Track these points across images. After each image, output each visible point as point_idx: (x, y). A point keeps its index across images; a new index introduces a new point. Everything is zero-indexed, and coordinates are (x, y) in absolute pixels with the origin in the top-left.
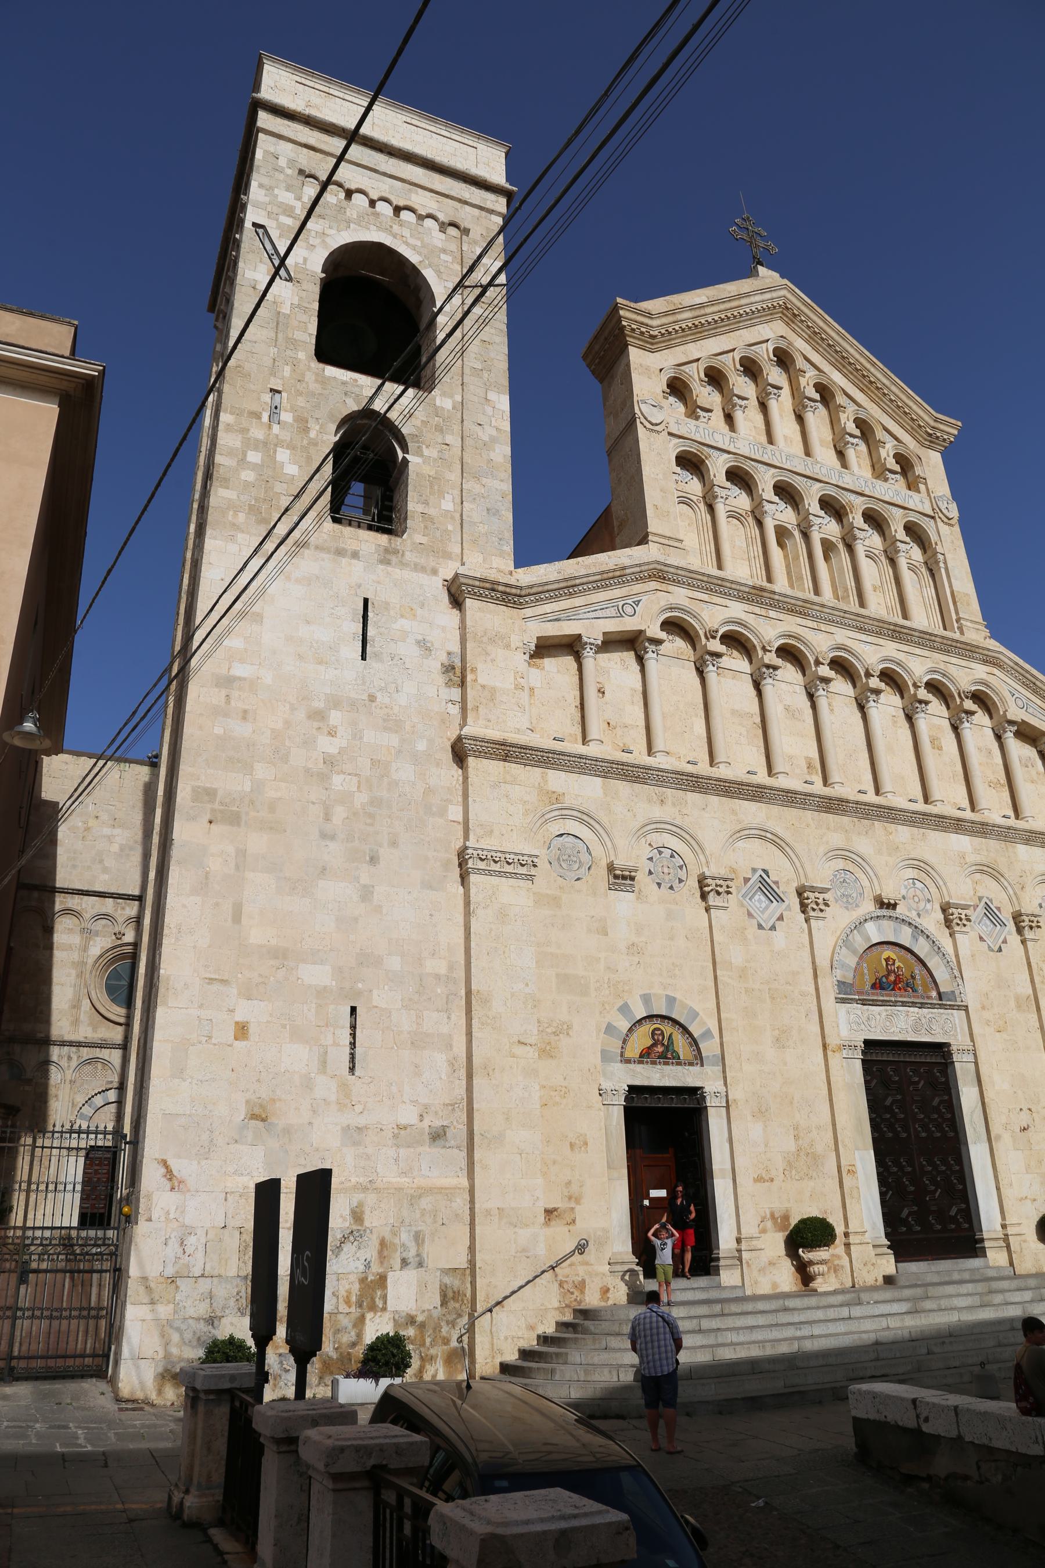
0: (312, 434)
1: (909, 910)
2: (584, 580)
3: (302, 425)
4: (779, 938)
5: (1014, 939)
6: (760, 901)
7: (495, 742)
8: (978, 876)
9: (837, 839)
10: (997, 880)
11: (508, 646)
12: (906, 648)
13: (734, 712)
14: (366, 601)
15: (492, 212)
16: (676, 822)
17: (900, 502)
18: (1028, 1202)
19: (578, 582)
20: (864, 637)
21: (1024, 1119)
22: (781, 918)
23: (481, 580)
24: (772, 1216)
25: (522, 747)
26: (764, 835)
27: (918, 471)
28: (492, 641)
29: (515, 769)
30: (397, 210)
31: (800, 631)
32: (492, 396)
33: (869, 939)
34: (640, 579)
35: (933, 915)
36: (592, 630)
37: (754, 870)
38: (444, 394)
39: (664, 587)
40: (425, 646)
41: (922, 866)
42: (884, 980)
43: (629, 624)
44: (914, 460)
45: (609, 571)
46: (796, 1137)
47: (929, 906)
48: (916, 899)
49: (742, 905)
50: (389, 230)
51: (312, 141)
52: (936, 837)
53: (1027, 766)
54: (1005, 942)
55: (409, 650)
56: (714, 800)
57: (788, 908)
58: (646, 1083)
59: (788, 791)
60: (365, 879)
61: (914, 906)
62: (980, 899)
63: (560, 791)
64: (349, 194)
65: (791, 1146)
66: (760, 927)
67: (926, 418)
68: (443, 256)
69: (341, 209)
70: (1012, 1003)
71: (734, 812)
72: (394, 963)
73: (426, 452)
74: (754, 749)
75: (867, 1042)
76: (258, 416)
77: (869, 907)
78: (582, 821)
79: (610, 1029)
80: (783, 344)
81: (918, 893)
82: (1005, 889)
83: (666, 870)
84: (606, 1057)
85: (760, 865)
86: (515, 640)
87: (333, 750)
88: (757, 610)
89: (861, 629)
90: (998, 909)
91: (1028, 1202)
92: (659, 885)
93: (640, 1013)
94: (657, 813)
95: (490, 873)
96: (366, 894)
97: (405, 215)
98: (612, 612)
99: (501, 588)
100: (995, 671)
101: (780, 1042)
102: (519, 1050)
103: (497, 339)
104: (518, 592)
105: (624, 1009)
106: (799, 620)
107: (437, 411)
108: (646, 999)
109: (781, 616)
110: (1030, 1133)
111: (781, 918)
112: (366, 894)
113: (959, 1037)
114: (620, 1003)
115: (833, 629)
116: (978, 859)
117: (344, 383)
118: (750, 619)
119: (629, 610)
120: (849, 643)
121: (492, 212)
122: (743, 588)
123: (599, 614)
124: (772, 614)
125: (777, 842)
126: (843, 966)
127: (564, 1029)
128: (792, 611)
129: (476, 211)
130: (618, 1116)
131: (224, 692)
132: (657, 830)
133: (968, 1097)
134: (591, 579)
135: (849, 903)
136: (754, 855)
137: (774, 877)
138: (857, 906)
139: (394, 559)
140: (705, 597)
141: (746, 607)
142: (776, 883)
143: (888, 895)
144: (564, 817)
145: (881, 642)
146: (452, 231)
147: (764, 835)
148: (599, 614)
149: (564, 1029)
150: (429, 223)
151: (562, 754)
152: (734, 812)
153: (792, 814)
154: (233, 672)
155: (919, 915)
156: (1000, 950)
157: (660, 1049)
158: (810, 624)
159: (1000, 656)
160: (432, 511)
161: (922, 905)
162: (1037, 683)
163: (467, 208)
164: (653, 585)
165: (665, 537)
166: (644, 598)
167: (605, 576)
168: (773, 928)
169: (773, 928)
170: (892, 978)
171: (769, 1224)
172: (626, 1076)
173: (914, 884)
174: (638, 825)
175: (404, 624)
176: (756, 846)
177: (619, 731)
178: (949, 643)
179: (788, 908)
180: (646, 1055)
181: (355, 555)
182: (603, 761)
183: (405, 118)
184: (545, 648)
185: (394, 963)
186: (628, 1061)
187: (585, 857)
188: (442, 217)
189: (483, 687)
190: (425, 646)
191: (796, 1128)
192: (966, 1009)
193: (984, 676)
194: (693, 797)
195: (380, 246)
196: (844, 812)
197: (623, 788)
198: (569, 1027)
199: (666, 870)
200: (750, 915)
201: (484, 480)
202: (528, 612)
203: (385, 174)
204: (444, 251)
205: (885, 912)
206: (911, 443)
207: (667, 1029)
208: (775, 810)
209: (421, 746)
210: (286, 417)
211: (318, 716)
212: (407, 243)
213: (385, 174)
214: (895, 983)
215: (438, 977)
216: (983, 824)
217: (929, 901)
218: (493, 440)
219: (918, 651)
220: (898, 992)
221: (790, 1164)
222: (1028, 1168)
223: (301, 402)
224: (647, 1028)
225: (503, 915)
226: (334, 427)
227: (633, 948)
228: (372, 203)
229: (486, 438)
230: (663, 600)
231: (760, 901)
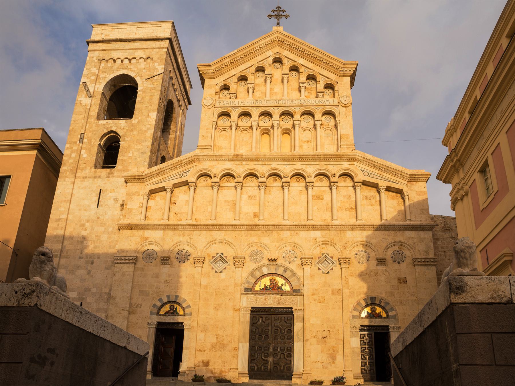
0: (92, 143)
1: (285, 261)
2: (166, 168)
3: (90, 141)
4: (223, 275)
5: (337, 268)
6: (220, 264)
7: (127, 225)
8: (324, 246)
9: (254, 239)
10: (334, 246)
11: (139, 195)
12: (307, 163)
13: (225, 201)
14: (101, 190)
15: (163, 48)
16: (188, 241)
17: (321, 104)
18: (319, 363)
19: (164, 169)
20: (286, 163)
21: (325, 334)
22: (225, 268)
23: (130, 176)
24: (203, 362)
25: (135, 225)
26: (223, 242)
27: (336, 89)
28: (134, 194)
29: (134, 232)
30: (130, 60)
31: (255, 167)
32: (150, 114)
33: (263, 273)
34: (189, 163)
35: (296, 262)
36: (168, 185)
37: (217, 254)
38: (136, 118)
39: (200, 164)
40: (116, 200)
41: (294, 245)
42: (268, 287)
43: (183, 179)
44: (335, 84)
45: (175, 163)
46: (217, 338)
47: (295, 259)
48: (290, 257)
49: (210, 265)
50: (127, 68)
51: (104, 48)
52: (303, 234)
53: (370, 199)
54: (332, 269)
55: (111, 202)
56: (204, 232)
57: (229, 265)
58: (164, 321)
59: (233, 225)
60: (89, 268)
61: (288, 260)
62: (322, 254)
63: (148, 236)
64: (115, 61)
65: (215, 341)
66: (216, 272)
67: (340, 65)
68: (144, 71)
69: (112, 67)
70: (330, 292)
71: (211, 235)
72: (94, 290)
73: (126, 139)
74: (232, 213)
75: (252, 308)
76: (76, 142)
77: (266, 262)
78: (155, 245)
79: (154, 306)
80: (277, 56)
81: (292, 256)
82: (337, 249)
83: (183, 257)
84: (152, 313)
85: (220, 251)
86: (141, 193)
87: (85, 234)
88: (237, 163)
89: (284, 160)
90: (332, 257)
91: (319, 363)
92: (180, 262)
93: (165, 300)
94: (181, 239)
95: (121, 263)
96: (89, 272)
97: (134, 61)
98: (179, 176)
99: (137, 177)
100: (355, 163)
101: (216, 309)
102: (122, 312)
103: (156, 94)
104: (142, 177)
105: (160, 300)
106: (256, 163)
107: (132, 125)
108: (168, 296)
109: (248, 163)
110: (326, 339)
111: (225, 268)
112: (89, 272)
113: (299, 305)
114: (159, 298)
115: (271, 163)
116: (324, 239)
117: (104, 125)
118: (234, 168)
119: (185, 174)
120: (277, 167)
121: (163, 48)
122: (230, 157)
123: (174, 178)
124: (244, 163)
125: (229, 243)
126: (248, 282)
127: (140, 306)
128: (252, 160)
129: (158, 50)
130: (153, 331)
131: (57, 223)
132: (182, 245)
133: (297, 326)
134: (169, 167)
135: (256, 261)
136: (216, 249)
137: (225, 255)
138: (260, 262)
139: (111, 176)
140: (216, 163)
141: (233, 163)
142: (226, 257)
143: (273, 257)
144: (149, 244)
145: (294, 163)
146: (149, 60)
147: (223, 242)
148: (174, 178)
149: (140, 306)
150: (142, 60)
151: (148, 225)
152: (211, 235)
153: (235, 233)
154: (61, 217)
155: (290, 263)
156: (328, 272)
157: (172, 311)
158: (260, 163)
159: (356, 157)
160: (125, 158)
161: (292, 259)
162: (375, 164)
163: (155, 50)
164: (195, 164)
165: (204, 146)
166: (191, 169)
167: (174, 165)
168: (221, 272)
169: (221, 272)
170: (272, 286)
171: (201, 364)
172: (155, 319)
173: (290, 252)
174: (173, 243)
175: (110, 194)
176: (220, 246)
177: (179, 215)
178: (328, 156)
179: (229, 265)
180: (167, 313)
181: (99, 177)
182: (162, 225)
183: (137, 26)
184: (152, 192)
185: (94, 290)
186: (161, 315)
187: (155, 256)
188: (144, 57)
189: (129, 209)
190: (116, 200)
191: (218, 335)
192: (303, 295)
193: (348, 166)
194: (196, 232)
195: (123, 74)
196: (259, 229)
197: (170, 233)
198: (141, 305)
199: (183, 257)
200: (213, 268)
201: (143, 144)
202: (147, 183)
203: (127, 49)
204: (144, 69)
205: (271, 262)
206: (333, 77)
207: (176, 305)
208: (229, 232)
209: (111, 229)
210: (85, 140)
211: (83, 225)
212: (132, 71)
213: (127, 49)
214: (273, 287)
215: (106, 293)
216: (326, 225)
217: (296, 257)
218: (148, 129)
219: (313, 163)
220: (274, 291)
221: (213, 347)
222: (322, 352)
223: (91, 134)
224: (168, 306)
225: (123, 274)
226: (98, 140)
227: (167, 282)
228: (122, 61)
229: (146, 129)
230: (199, 168)
231: (220, 264)
